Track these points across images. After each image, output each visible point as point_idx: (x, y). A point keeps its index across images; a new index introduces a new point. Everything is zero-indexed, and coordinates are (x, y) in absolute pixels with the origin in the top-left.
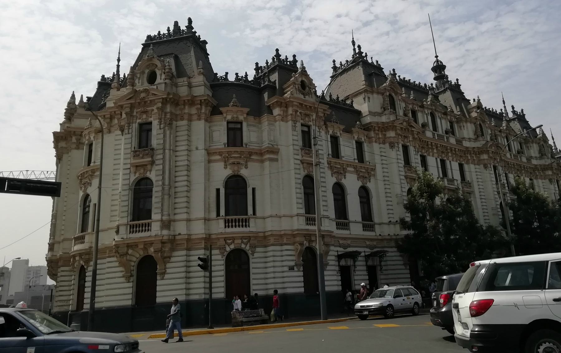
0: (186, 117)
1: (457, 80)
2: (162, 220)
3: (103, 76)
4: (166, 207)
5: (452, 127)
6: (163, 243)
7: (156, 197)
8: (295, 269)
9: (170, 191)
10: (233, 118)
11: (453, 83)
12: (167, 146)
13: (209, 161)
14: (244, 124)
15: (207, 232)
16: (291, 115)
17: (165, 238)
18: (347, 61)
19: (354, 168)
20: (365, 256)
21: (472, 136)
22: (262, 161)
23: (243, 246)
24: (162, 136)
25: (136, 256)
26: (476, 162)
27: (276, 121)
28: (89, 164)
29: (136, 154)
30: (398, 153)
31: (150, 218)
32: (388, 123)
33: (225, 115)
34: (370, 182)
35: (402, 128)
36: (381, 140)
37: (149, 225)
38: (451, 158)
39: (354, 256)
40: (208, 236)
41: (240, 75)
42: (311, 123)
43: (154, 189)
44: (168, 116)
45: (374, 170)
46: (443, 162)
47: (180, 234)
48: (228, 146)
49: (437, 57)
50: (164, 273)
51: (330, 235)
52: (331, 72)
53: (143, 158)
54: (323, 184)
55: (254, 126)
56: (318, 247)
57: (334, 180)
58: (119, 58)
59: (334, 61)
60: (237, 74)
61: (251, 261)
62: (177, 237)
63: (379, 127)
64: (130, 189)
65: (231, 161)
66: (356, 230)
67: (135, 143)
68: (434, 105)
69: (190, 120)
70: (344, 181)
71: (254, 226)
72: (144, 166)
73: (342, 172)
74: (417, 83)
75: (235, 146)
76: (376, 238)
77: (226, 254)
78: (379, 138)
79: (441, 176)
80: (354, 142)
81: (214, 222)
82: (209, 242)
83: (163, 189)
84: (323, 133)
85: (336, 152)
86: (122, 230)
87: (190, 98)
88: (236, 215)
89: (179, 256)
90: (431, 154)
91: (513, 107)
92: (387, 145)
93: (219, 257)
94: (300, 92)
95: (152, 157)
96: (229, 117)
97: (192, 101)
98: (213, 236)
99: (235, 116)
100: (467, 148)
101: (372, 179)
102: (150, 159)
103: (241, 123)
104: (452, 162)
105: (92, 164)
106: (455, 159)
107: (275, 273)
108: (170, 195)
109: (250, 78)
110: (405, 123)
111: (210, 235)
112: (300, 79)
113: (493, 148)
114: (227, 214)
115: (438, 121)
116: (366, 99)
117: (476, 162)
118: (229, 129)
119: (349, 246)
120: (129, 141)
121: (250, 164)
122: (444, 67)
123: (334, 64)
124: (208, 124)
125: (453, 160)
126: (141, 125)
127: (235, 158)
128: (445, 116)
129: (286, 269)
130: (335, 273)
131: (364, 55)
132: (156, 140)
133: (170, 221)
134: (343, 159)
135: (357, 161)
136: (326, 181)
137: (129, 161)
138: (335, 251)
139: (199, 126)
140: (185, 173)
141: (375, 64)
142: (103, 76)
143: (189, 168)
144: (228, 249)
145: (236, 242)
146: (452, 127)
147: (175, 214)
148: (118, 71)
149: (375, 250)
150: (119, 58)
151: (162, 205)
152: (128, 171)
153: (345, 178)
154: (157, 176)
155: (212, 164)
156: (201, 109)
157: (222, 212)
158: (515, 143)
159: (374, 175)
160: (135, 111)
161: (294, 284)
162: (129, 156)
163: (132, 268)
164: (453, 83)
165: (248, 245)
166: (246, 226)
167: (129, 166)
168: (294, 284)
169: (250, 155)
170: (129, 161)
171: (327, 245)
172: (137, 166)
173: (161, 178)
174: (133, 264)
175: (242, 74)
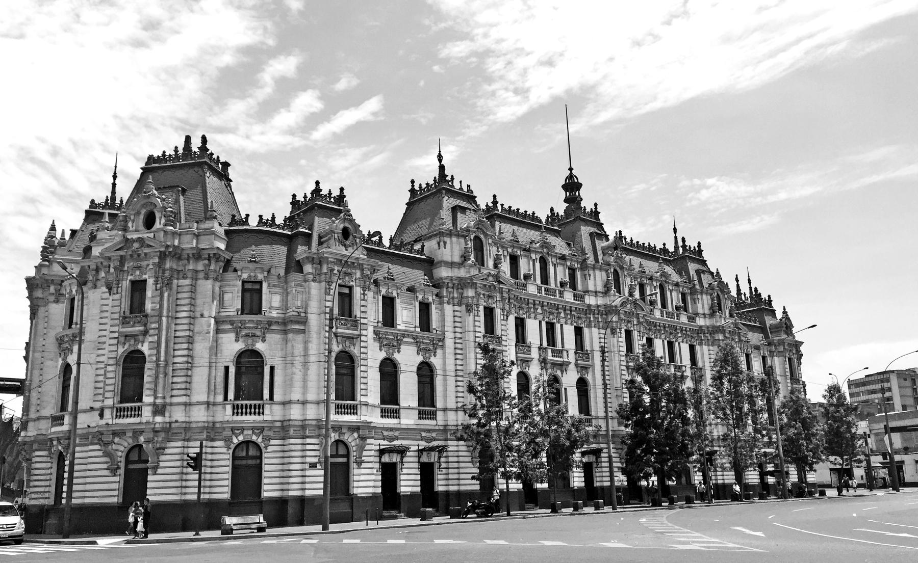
0: (189, 274)
1: (596, 205)
2: (154, 404)
3: (93, 202)
4: (160, 389)
5: (572, 276)
6: (156, 432)
8: (319, 466)
9: (165, 367)
10: (250, 276)
11: (588, 210)
12: (165, 313)
13: (218, 331)
14: (265, 285)
15: (211, 419)
16: (326, 274)
17: (157, 426)
18: (427, 184)
19: (413, 338)
20: (419, 451)
21: (600, 288)
22: (285, 332)
23: (254, 438)
24: (158, 299)
25: (121, 447)
26: (601, 325)
27: (305, 281)
28: (70, 327)
29: (125, 321)
30: (477, 318)
31: (140, 400)
32: (465, 279)
33: (239, 273)
34: (435, 355)
35: (485, 286)
36: (456, 301)
37: (140, 409)
38: (562, 321)
39: (402, 451)
40: (211, 425)
41: (265, 218)
42: (354, 284)
43: (147, 366)
44: (167, 274)
45: (442, 339)
46: (551, 327)
47: (176, 421)
48: (242, 313)
49: (571, 169)
50: (155, 468)
51: (368, 426)
52: (407, 196)
53: (133, 326)
54: (363, 362)
55: (276, 286)
56: (351, 439)
57: (383, 355)
58: (115, 173)
59: (413, 182)
60: (260, 216)
61: (264, 455)
62: (173, 425)
63: (454, 284)
64: (117, 364)
65: (244, 332)
66: (409, 419)
67: (126, 305)
68: (546, 247)
69: (195, 279)
70: (397, 356)
71: (272, 413)
72: (134, 336)
73: (395, 344)
74: (530, 212)
75: (251, 313)
76: (437, 428)
77: (233, 446)
78: (453, 298)
79: (545, 344)
80: (417, 304)
81: (220, 408)
82: (212, 431)
83: (158, 365)
84: (370, 295)
85: (389, 318)
86: (107, 413)
87: (195, 252)
88: (248, 400)
89: (174, 447)
90: (533, 315)
91: (683, 240)
92: (464, 307)
93: (224, 450)
94: (341, 242)
95: (145, 325)
96: (245, 276)
97: (198, 255)
98: (218, 425)
99: (252, 274)
100: (589, 306)
101: (439, 351)
102: (142, 328)
103: (261, 283)
104: (564, 326)
105: (73, 326)
106: (569, 321)
107: (293, 472)
108: (166, 375)
109: (279, 221)
110: (491, 278)
111: (214, 423)
112: (342, 226)
113: (629, 306)
114: (236, 398)
115: (551, 269)
116: (442, 243)
117: (601, 325)
118: (244, 291)
119: (396, 438)
120: (117, 303)
121: (268, 336)
122: (579, 186)
123: (413, 186)
124: (218, 284)
125: (566, 323)
126: (133, 283)
127: (250, 328)
128: (562, 262)
129: (307, 466)
130: (375, 471)
131: (449, 178)
133: (164, 406)
134: (399, 327)
135: (418, 330)
136: (371, 356)
137: (116, 329)
138: (373, 445)
139: (206, 286)
140: (185, 346)
141: (465, 189)
142: (93, 202)
143: (190, 340)
144: (235, 441)
145: (245, 432)
146: (572, 276)
147: (172, 396)
148: (113, 192)
149: (435, 443)
150: (115, 173)
151: (156, 386)
152: (115, 341)
153: (399, 352)
154: (150, 349)
155: (220, 336)
156: (209, 265)
157: (231, 396)
158: (674, 294)
159: (443, 347)
160: (126, 265)
161: (315, 485)
162: (116, 322)
163: (119, 459)
164: (588, 210)
165: (261, 437)
166: (259, 414)
167: (116, 335)
168: (315, 485)
169: (270, 325)
170: (116, 329)
171: (363, 439)
172: (126, 336)
173: (155, 352)
174: (120, 454)
175: (267, 216)
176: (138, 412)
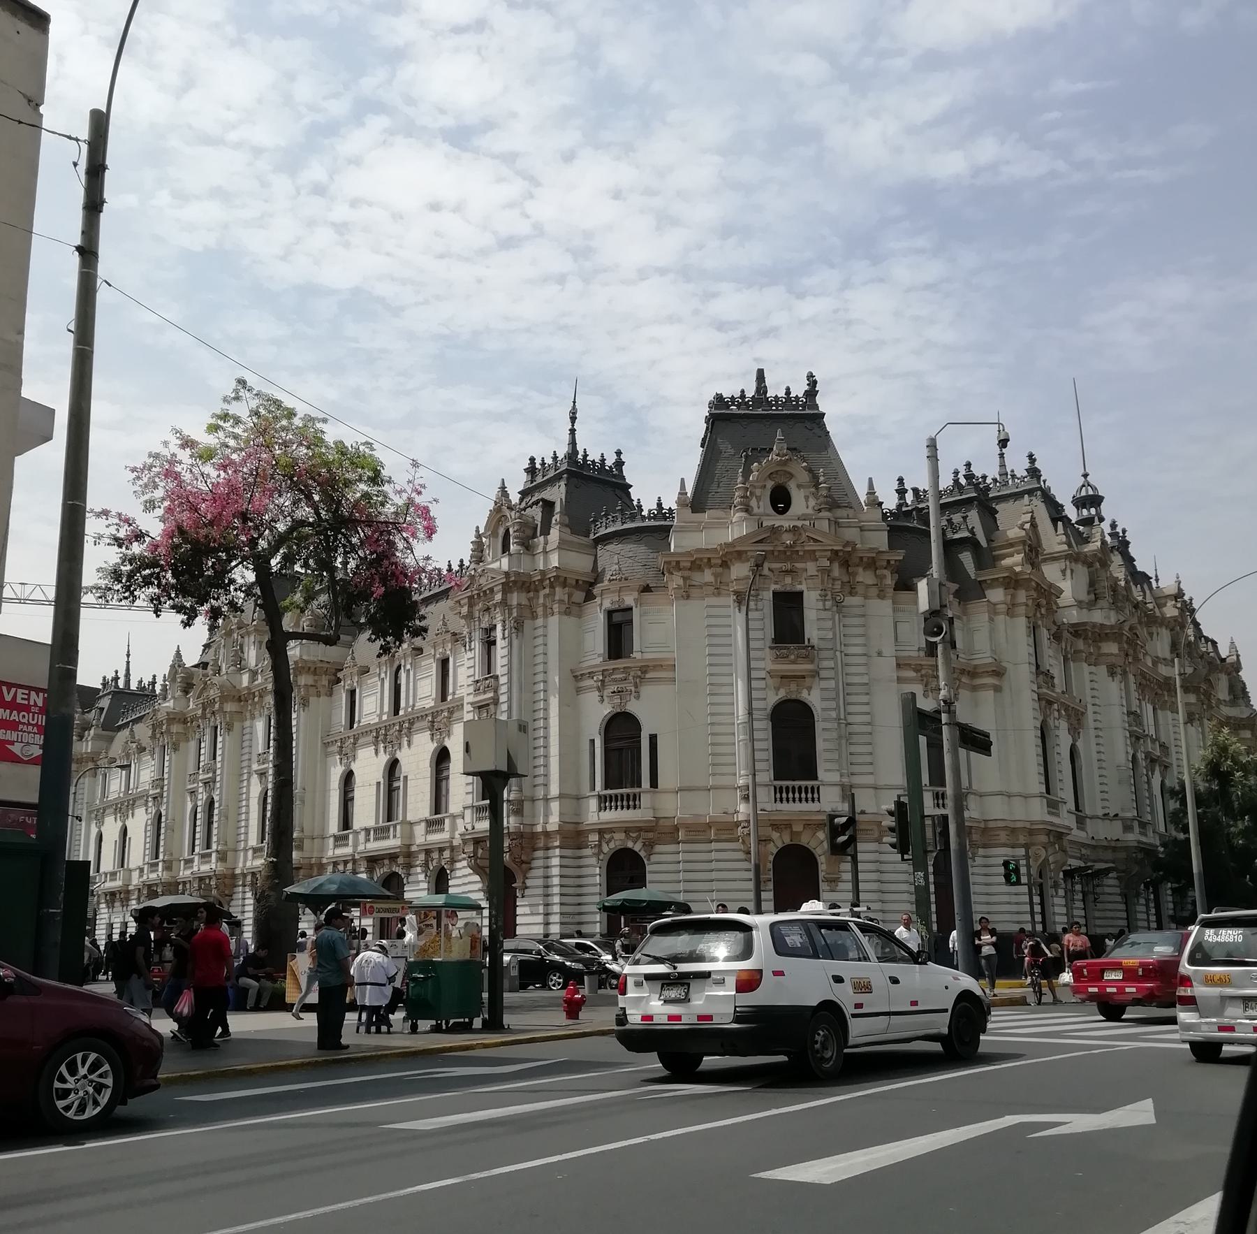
0: (860, 589)
7: (825, 740)
47: (863, 812)
53: (793, 662)
72: (799, 678)
126: (775, 594)
132: (814, 629)
151: (840, 756)
154: (823, 699)
176: (813, 794)
